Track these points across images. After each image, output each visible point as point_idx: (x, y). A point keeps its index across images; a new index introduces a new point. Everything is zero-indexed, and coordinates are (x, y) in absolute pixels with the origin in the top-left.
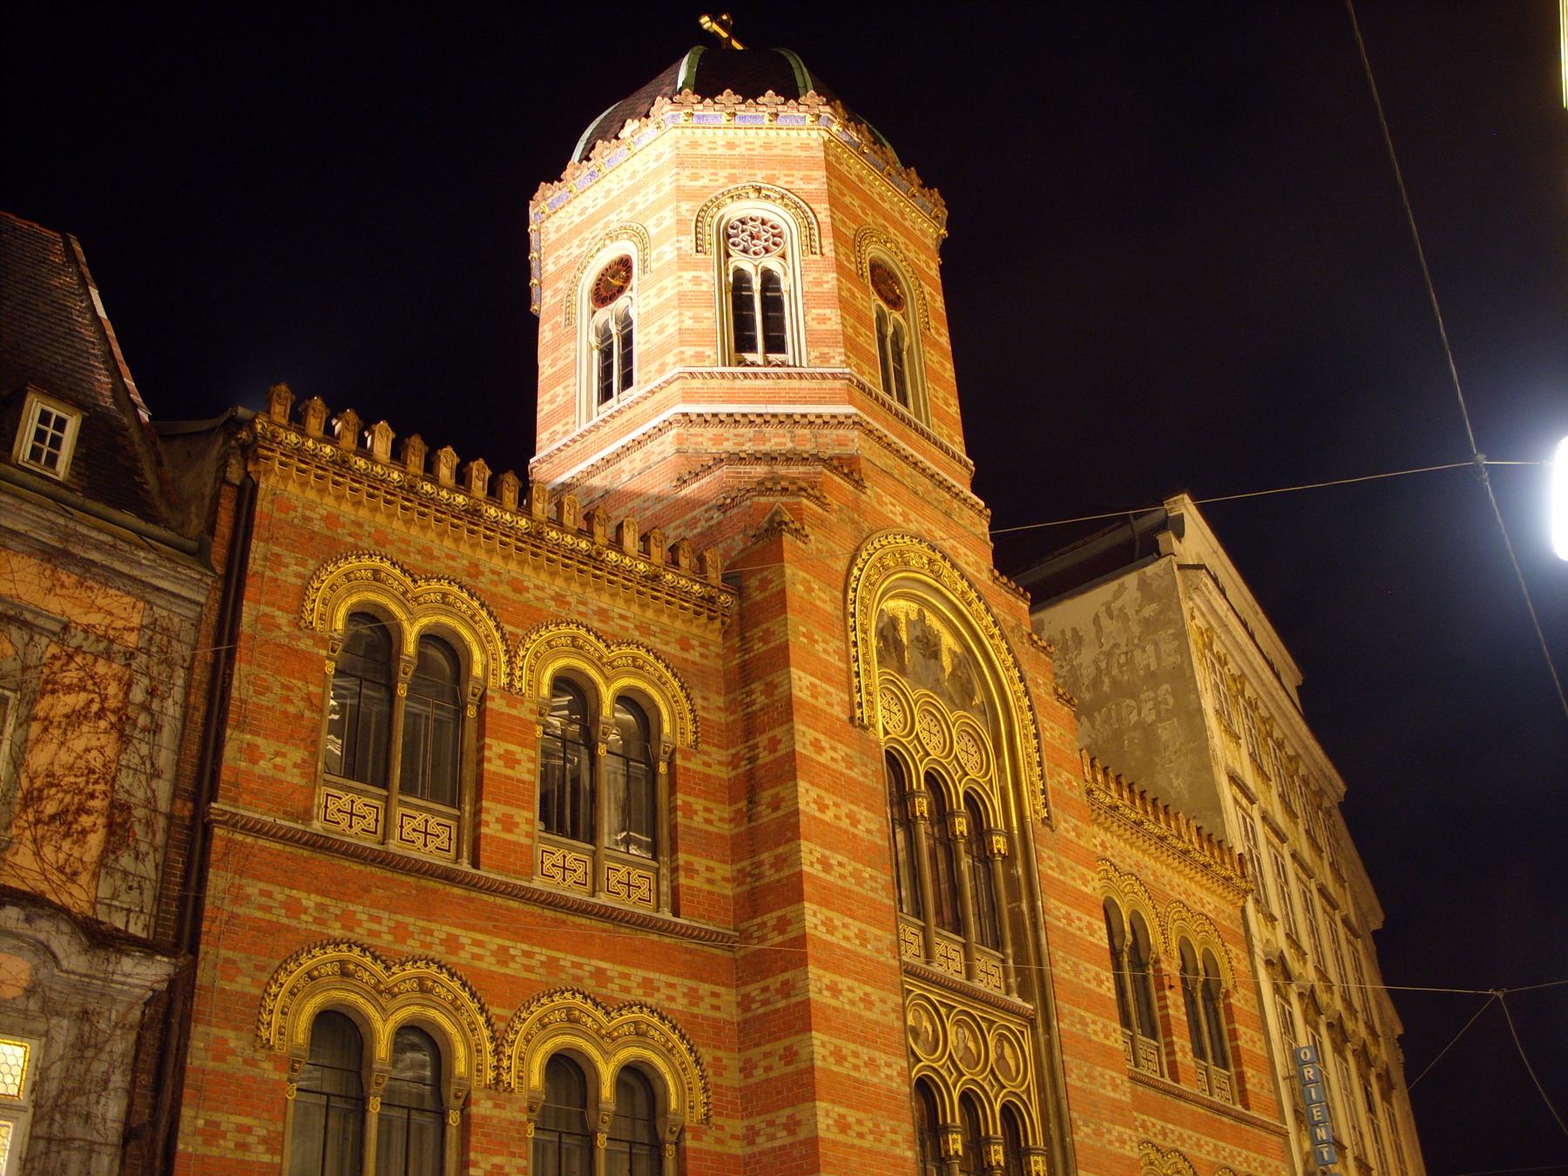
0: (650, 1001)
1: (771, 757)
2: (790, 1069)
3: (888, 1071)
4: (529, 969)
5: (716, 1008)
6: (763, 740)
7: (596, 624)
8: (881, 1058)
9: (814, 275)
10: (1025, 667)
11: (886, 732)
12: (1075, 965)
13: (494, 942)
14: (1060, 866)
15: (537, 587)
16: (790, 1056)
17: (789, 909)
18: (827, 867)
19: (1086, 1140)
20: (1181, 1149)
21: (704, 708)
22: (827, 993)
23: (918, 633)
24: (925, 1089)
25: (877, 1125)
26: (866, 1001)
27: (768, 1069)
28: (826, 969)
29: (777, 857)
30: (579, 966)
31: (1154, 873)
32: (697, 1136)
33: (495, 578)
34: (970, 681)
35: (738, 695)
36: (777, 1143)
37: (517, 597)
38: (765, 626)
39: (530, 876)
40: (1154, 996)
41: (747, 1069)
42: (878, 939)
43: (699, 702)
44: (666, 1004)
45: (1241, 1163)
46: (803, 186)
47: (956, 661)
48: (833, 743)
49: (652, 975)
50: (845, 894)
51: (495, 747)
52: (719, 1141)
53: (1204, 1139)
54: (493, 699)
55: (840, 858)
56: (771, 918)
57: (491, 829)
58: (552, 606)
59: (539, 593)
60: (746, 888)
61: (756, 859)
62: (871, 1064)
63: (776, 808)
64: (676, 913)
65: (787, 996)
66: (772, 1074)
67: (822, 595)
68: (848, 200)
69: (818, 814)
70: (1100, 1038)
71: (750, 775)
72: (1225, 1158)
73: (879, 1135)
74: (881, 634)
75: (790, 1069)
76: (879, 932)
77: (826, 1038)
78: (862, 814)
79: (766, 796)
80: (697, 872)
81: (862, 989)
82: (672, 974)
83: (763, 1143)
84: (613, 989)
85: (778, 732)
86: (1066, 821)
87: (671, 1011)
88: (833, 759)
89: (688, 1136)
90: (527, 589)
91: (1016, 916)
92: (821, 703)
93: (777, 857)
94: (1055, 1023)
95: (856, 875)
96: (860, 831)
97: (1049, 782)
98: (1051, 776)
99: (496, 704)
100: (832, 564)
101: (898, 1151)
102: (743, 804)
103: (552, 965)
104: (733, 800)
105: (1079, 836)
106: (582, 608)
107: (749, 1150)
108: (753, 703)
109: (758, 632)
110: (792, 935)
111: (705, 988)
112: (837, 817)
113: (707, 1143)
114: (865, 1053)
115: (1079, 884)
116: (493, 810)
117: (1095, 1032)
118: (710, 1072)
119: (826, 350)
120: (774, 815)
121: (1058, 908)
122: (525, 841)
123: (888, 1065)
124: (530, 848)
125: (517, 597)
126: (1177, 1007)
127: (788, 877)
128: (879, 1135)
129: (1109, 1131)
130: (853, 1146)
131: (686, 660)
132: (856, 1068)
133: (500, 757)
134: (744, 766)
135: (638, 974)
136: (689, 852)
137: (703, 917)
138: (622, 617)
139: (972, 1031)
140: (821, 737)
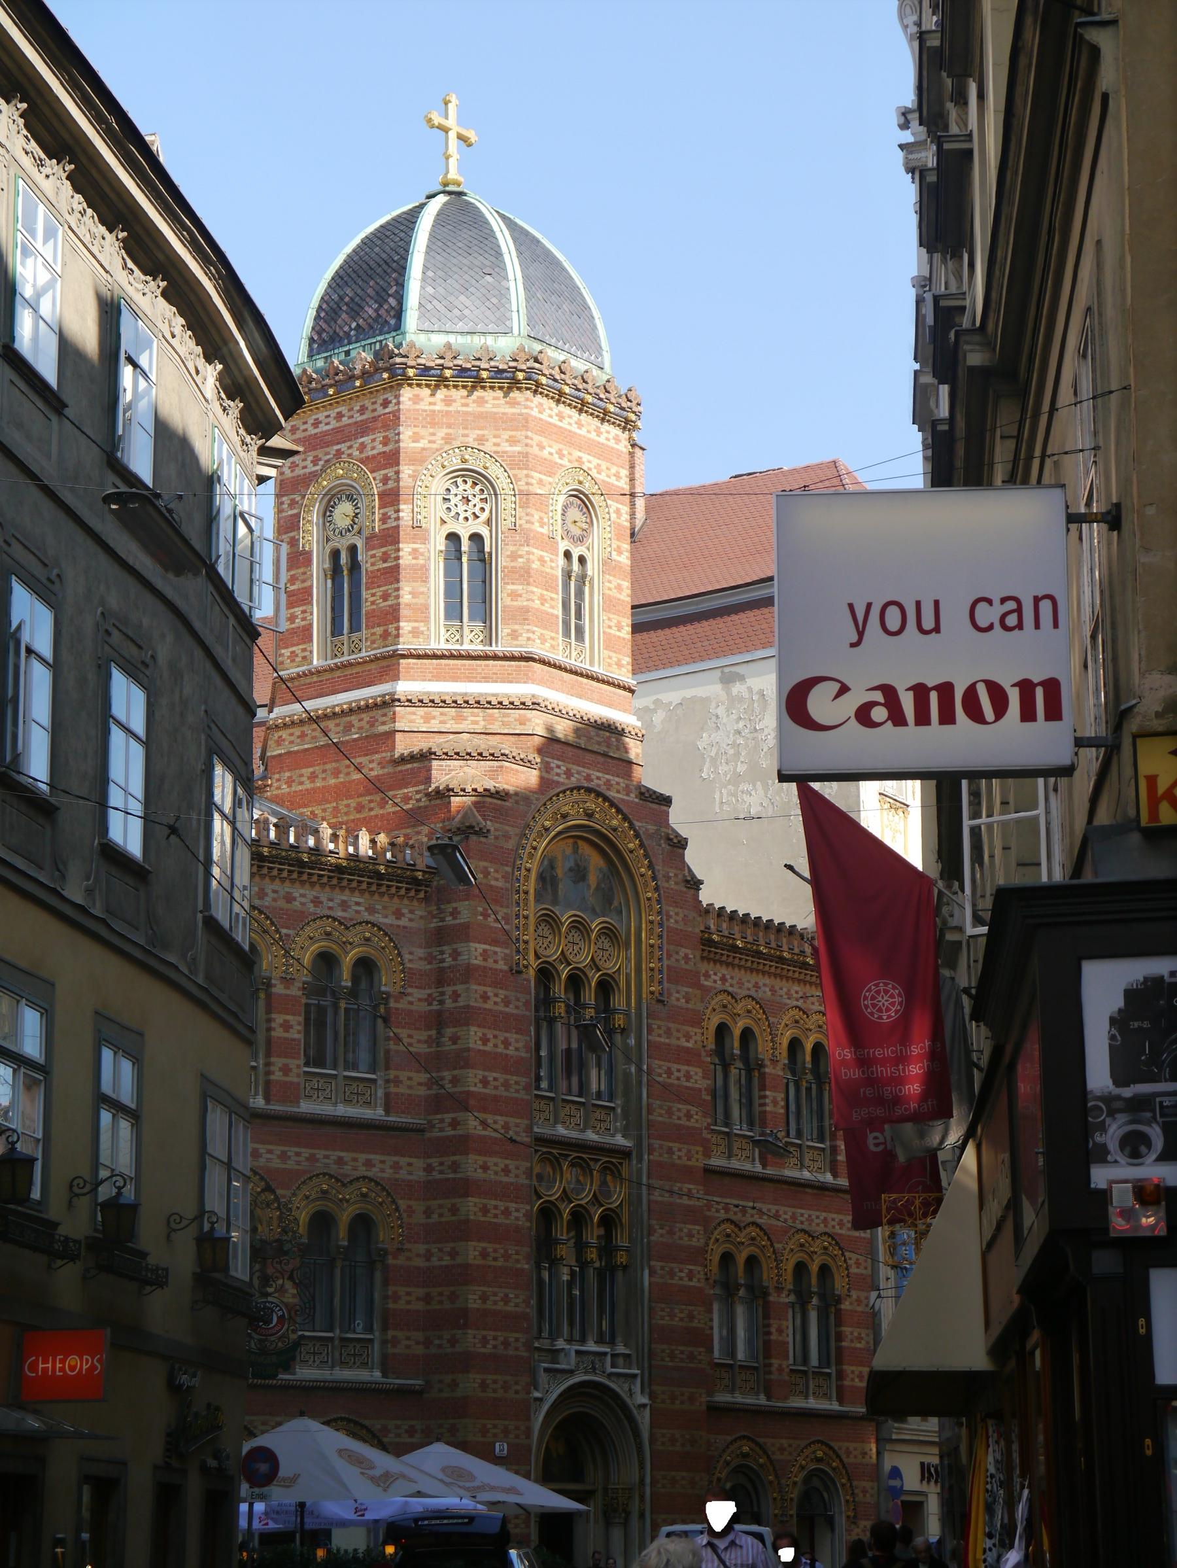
0: (370, 1174)
1: (454, 1005)
2: (453, 1218)
3: (516, 1214)
4: (298, 1163)
5: (410, 1173)
6: (449, 990)
7: (339, 914)
8: (513, 1206)
9: (512, 548)
10: (657, 867)
11: (537, 956)
12: (670, 1108)
13: (278, 1149)
14: (668, 1032)
15: (302, 896)
16: (454, 1210)
17: (461, 1114)
18: (485, 1082)
20: (759, 1221)
21: (410, 961)
22: (480, 1171)
23: (571, 864)
24: (547, 1214)
25: (506, 1251)
26: (506, 1171)
27: (441, 1215)
28: (480, 1154)
29: (454, 1077)
30: (326, 1157)
31: (773, 990)
32: (395, 1258)
33: (275, 895)
34: (611, 889)
35: (435, 951)
36: (444, 1263)
37: (288, 906)
38: (454, 905)
39: (296, 1101)
40: (756, 1093)
41: (428, 1212)
42: (517, 1125)
43: (407, 957)
44: (380, 1174)
45: (818, 1225)
46: (509, 449)
48: (496, 991)
49: (371, 1156)
50: (496, 1099)
51: (279, 1018)
52: (409, 1259)
53: (782, 1209)
54: (275, 986)
55: (495, 1075)
56: (448, 1117)
57: (277, 1076)
58: (311, 908)
59: (303, 900)
60: (433, 1092)
61: (440, 1074)
62: (506, 1213)
63: (455, 1043)
64: (387, 1111)
65: (455, 1172)
66: (443, 1219)
67: (496, 875)
68: (545, 453)
69: (482, 1048)
70: (684, 1161)
71: (439, 1013)
72: (802, 1223)
73: (507, 1257)
74: (541, 878)
75: (453, 1218)
76: (518, 1121)
77: (477, 1200)
78: (512, 1037)
79: (449, 1031)
80: (401, 1082)
81: (502, 1162)
82: (383, 1154)
83: (435, 1261)
84: (347, 1169)
85: (460, 988)
86: (678, 992)
87: (383, 1179)
88: (496, 1003)
89: (390, 1257)
90: (295, 899)
91: (627, 1075)
92: (490, 963)
93: (454, 1077)
95: (506, 1085)
96: (511, 1051)
97: (666, 962)
98: (669, 956)
99: (279, 989)
101: (519, 1266)
102: (433, 1032)
103: (312, 1159)
104: (428, 1027)
105: (687, 1002)
106: (331, 904)
107: (427, 1264)
108: (443, 961)
109: (449, 908)
110: (461, 1132)
111: (403, 1161)
112: (495, 1046)
113: (401, 1261)
114: (502, 1205)
116: (278, 1062)
117: (680, 1158)
118: (405, 1215)
119: (516, 627)
120: (453, 1047)
121: (660, 1067)
122: (295, 1080)
123: (517, 1210)
124: (299, 1084)
125: (288, 906)
126: (775, 1103)
127: (461, 1093)
128: (507, 1257)
129: (681, 1230)
130: (489, 1267)
131: (398, 926)
132: (496, 1216)
133: (281, 1025)
134: (435, 1007)
135: (362, 1157)
136: (396, 1069)
137: (403, 1112)
138: (357, 904)
140: (488, 989)
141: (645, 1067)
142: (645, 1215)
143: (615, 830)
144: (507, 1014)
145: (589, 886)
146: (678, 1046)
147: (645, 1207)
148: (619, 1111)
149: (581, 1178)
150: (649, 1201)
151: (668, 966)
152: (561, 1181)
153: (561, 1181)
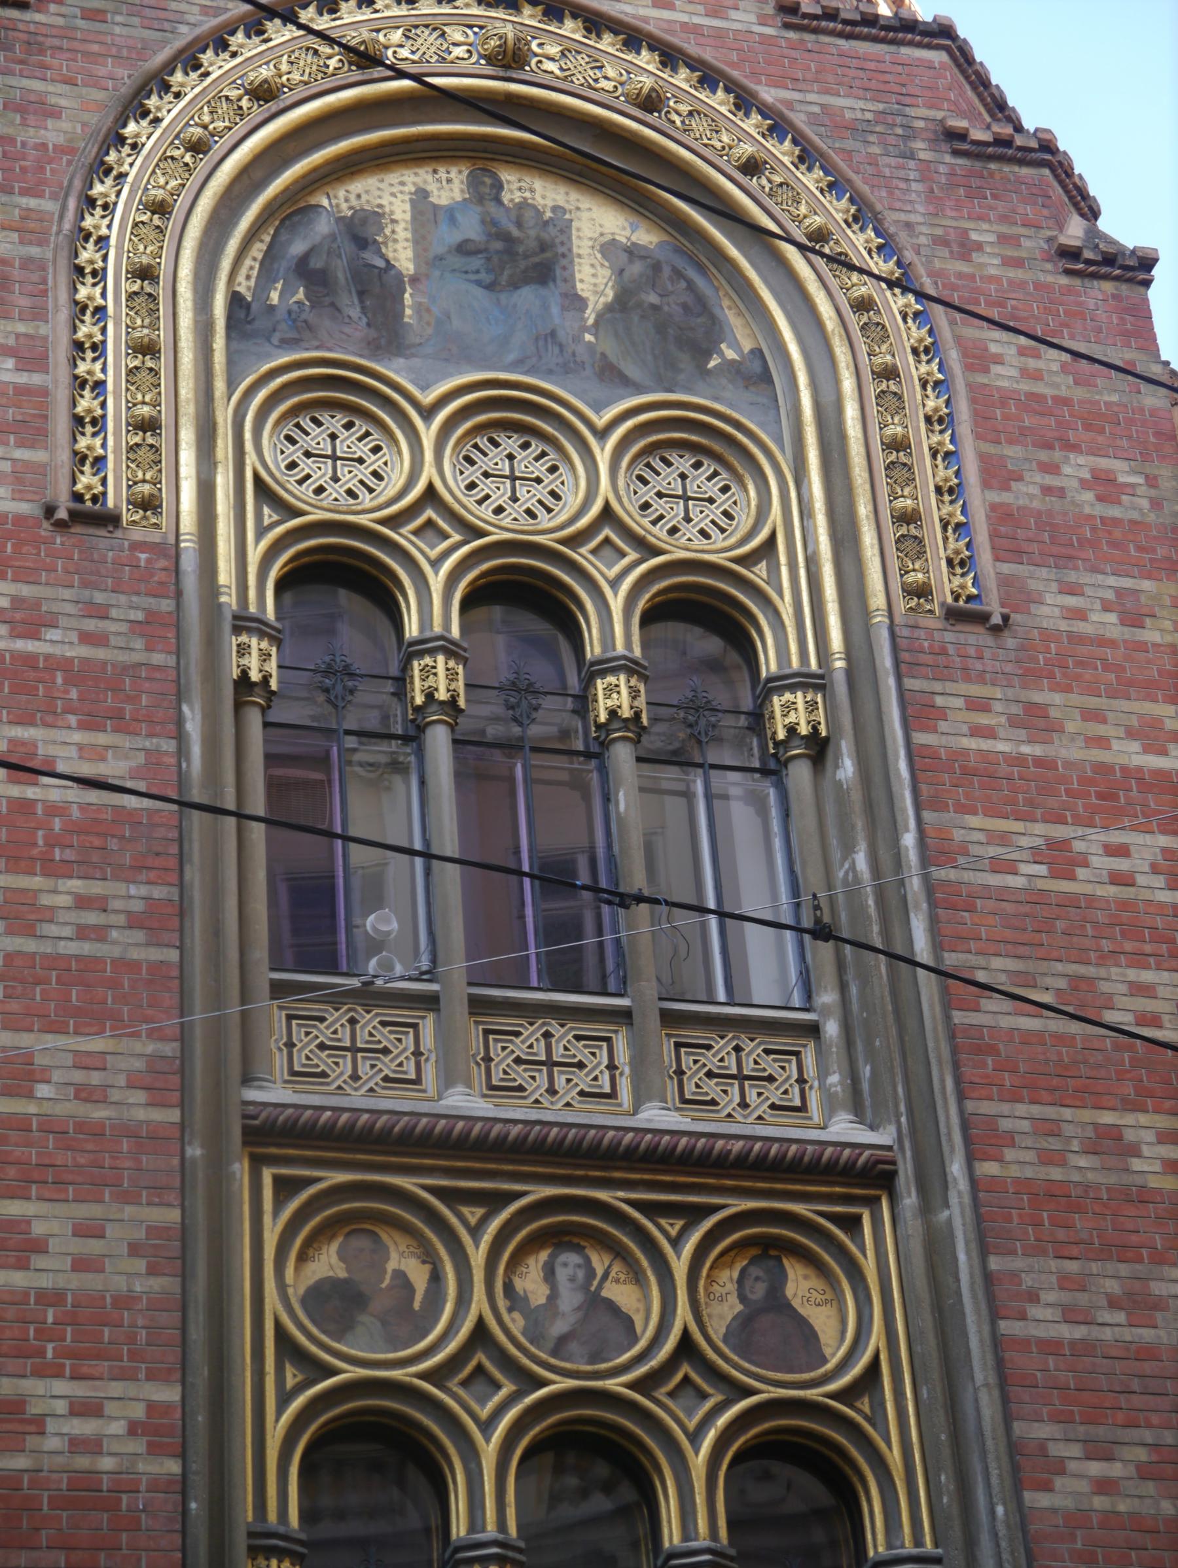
19: (1099, 1502)
23: (470, 228)
34: (701, 307)
47: (637, 268)
94: (956, 1168)
100: (30, 136)
105: (1133, 619)
115: (1130, 754)
139: (618, 1252)
141: (909, 840)
142: (988, 1407)
143: (650, 103)
144: (29, 660)
145: (577, 302)
146: (1104, 769)
147: (981, 1371)
148: (831, 1029)
149: (622, 1294)
150: (997, 1343)
151: (1001, 516)
152: (463, 1300)
153: (463, 1300)
